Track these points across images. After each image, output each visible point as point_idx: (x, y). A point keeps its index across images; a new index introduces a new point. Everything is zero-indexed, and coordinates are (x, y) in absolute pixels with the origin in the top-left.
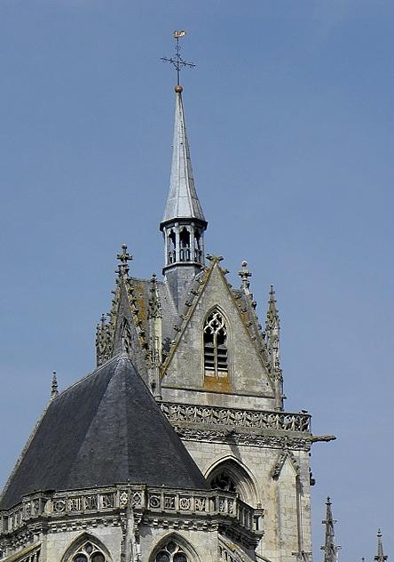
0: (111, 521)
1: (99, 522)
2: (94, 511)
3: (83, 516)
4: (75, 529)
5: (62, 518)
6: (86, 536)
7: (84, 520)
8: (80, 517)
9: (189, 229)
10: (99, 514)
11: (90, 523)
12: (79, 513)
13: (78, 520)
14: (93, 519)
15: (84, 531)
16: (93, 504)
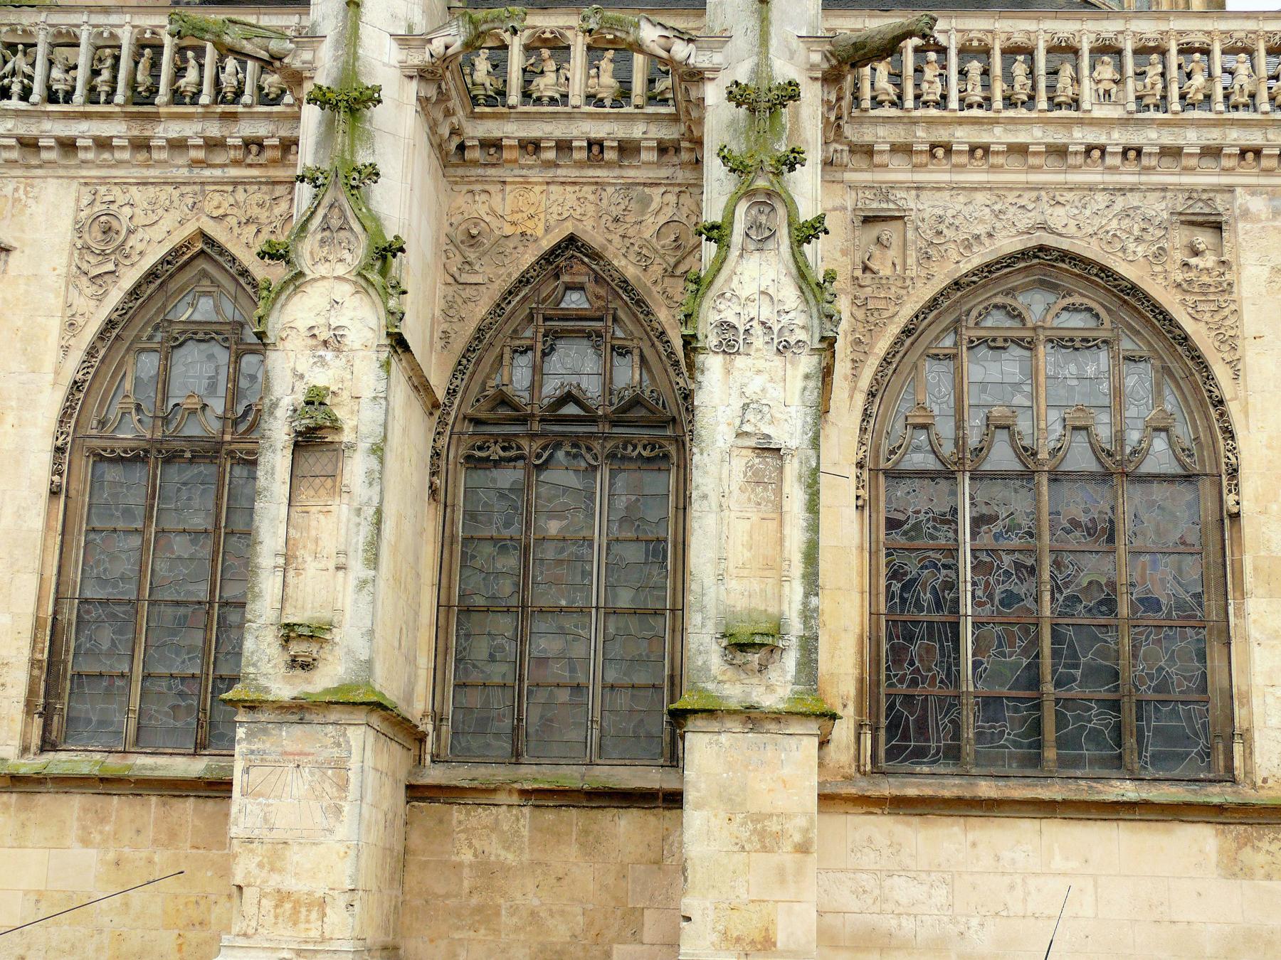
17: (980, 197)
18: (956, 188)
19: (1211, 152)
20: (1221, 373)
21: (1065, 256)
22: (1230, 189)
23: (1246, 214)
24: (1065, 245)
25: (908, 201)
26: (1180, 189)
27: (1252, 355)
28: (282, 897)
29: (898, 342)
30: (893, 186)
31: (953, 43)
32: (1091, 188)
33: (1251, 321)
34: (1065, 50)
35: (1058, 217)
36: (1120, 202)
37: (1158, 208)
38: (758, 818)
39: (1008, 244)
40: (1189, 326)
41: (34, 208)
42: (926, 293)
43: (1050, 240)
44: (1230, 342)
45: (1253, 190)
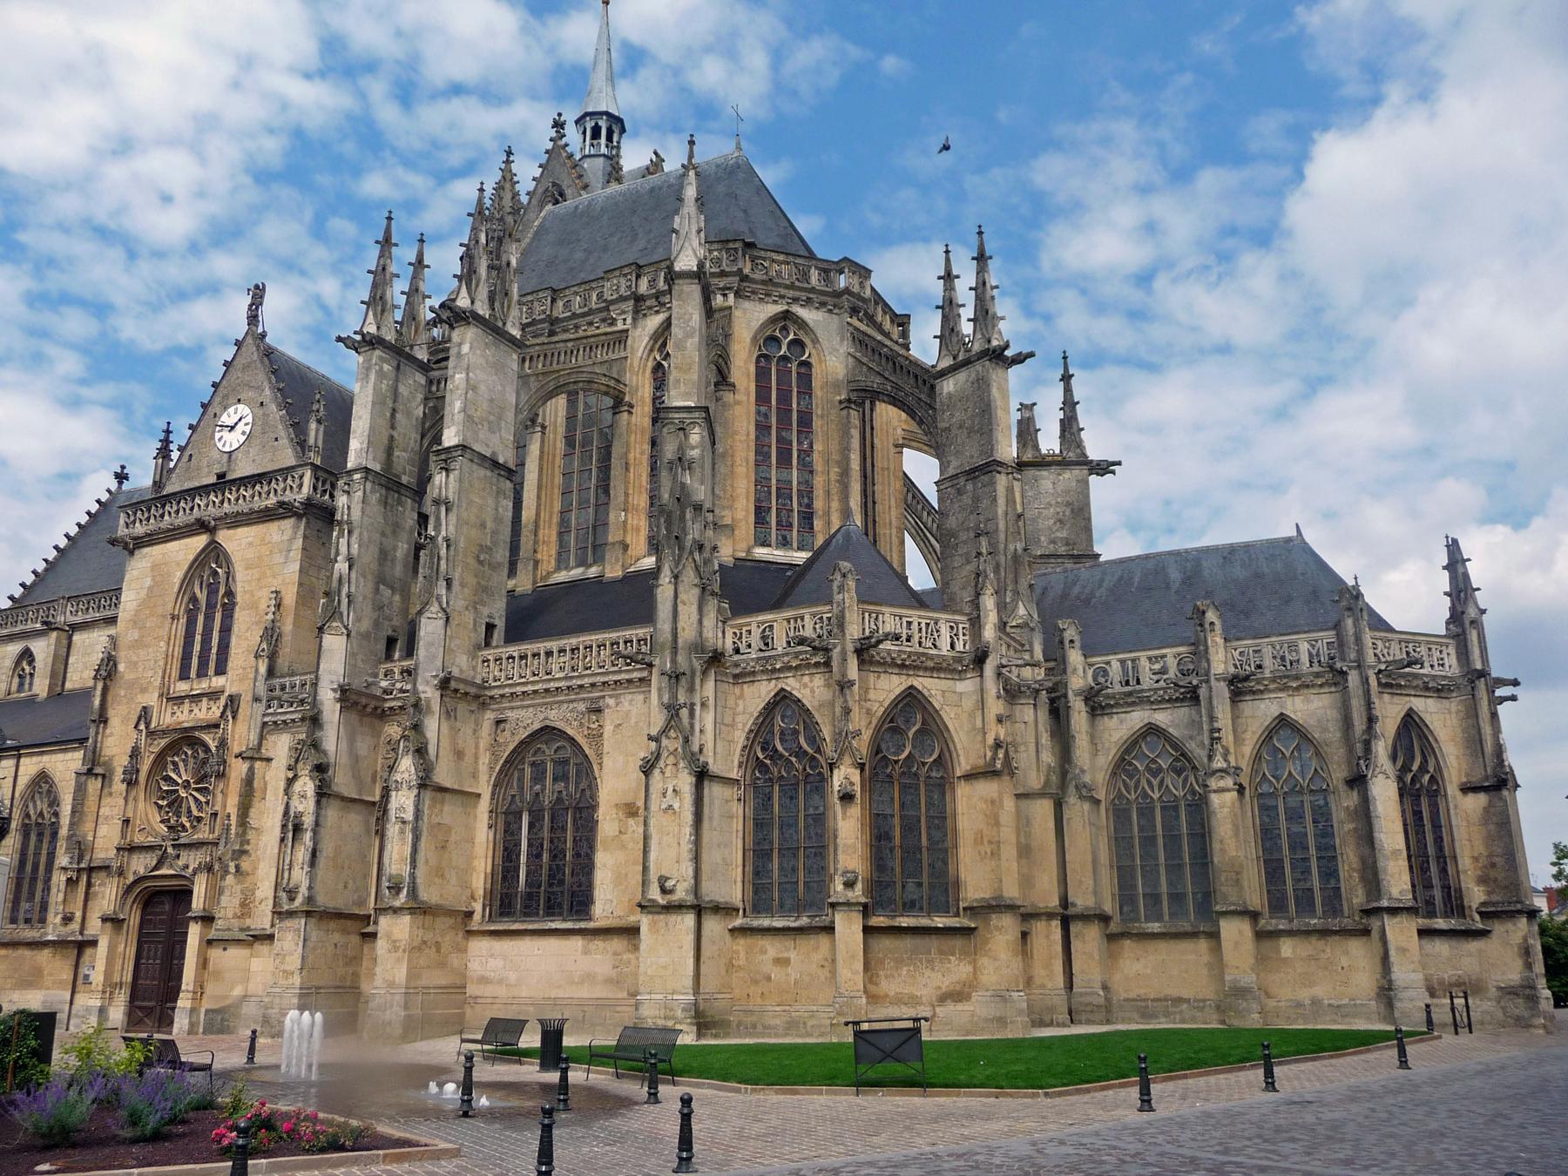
0: (823, 304)
1: (809, 301)
2: (806, 285)
3: (791, 287)
4: (775, 302)
5: (763, 282)
6: (786, 316)
7: (791, 293)
8: (787, 287)
9: (614, 127)
10: (813, 290)
11: (795, 300)
12: (788, 282)
13: (783, 291)
14: (804, 295)
15: (785, 307)
16: (805, 277)
17: (531, 710)
18: (523, 707)
19: (593, 685)
20: (595, 767)
21: (554, 728)
22: (604, 697)
23: (608, 706)
24: (553, 724)
25: (509, 714)
26: (588, 699)
27: (607, 761)
28: (284, 971)
29: (503, 766)
30: (505, 709)
31: (516, 654)
32: (562, 702)
33: (606, 749)
34: (549, 654)
35: (553, 714)
36: (571, 706)
37: (582, 707)
38: (395, 941)
39: (537, 726)
40: (587, 751)
41: (279, 743)
42: (511, 747)
43: (548, 723)
44: (600, 755)
45: (611, 696)
